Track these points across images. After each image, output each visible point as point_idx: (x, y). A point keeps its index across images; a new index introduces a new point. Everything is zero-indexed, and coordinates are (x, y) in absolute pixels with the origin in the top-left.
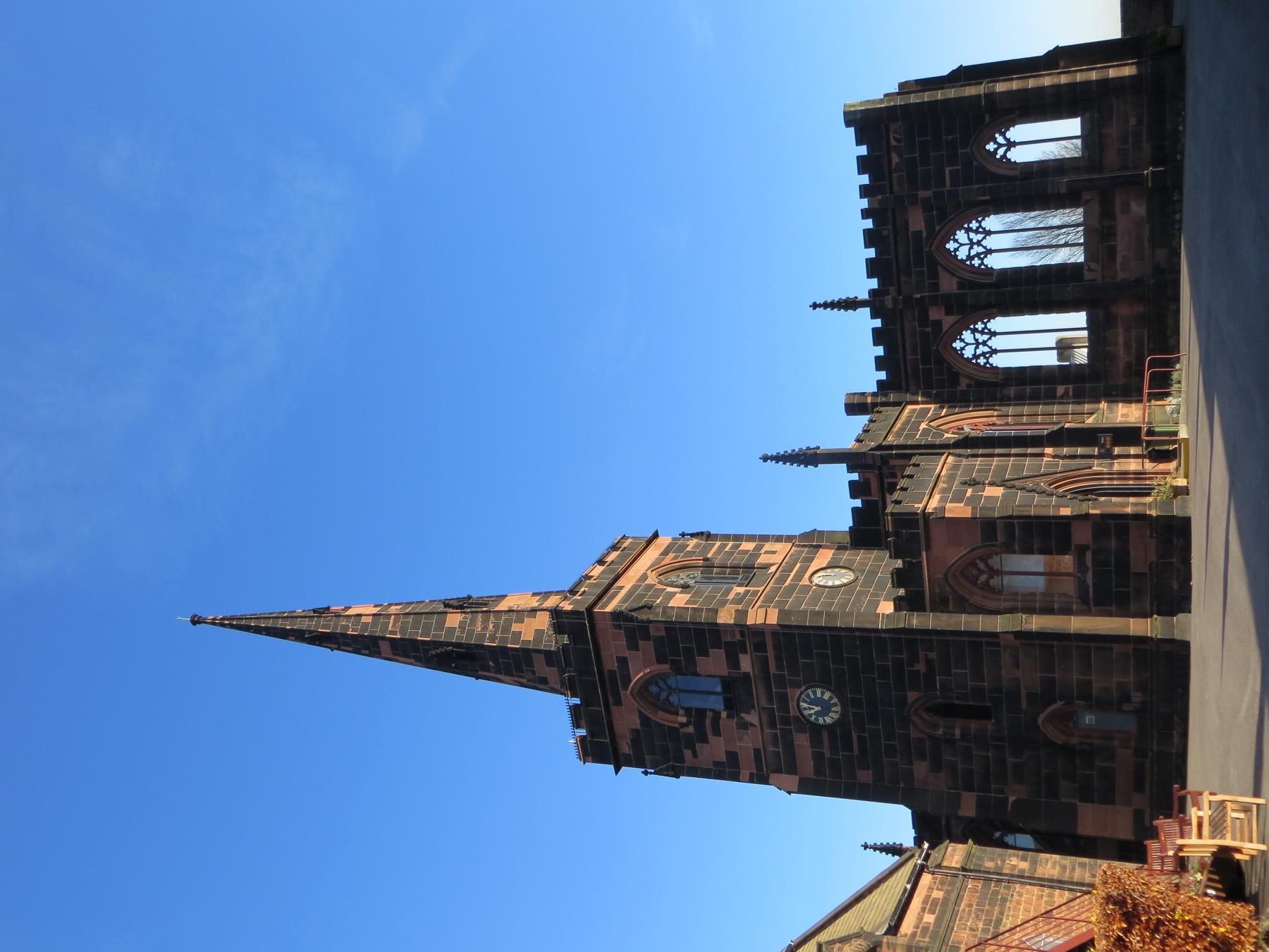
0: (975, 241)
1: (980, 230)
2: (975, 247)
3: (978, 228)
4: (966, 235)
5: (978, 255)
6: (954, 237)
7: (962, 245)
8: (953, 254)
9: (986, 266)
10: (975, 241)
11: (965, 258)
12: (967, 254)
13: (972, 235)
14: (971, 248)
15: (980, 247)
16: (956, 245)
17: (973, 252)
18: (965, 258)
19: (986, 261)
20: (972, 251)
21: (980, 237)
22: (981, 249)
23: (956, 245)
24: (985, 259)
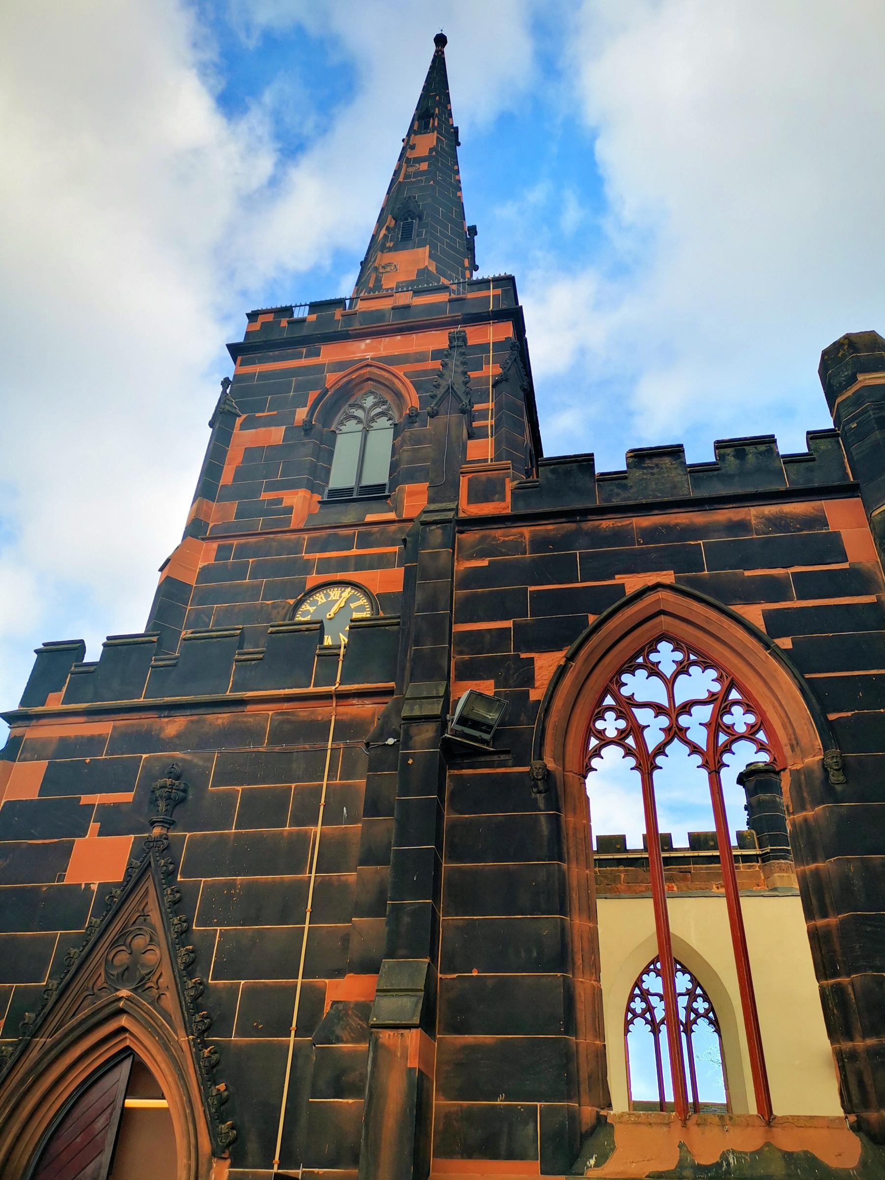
0: (684, 721)
1: (723, 738)
2: (664, 721)
3: (729, 729)
4: (704, 696)
5: (637, 730)
6: (694, 663)
7: (670, 684)
8: (640, 660)
9: (597, 753)
10: (684, 721)
11: (625, 692)
12: (639, 698)
13: (703, 713)
14: (659, 710)
15: (662, 737)
16: (668, 669)
17: (643, 716)
18: (625, 692)
19: (612, 753)
20: (650, 712)
21: (699, 737)
22: (653, 738)
23: (668, 669)
24: (621, 751)
